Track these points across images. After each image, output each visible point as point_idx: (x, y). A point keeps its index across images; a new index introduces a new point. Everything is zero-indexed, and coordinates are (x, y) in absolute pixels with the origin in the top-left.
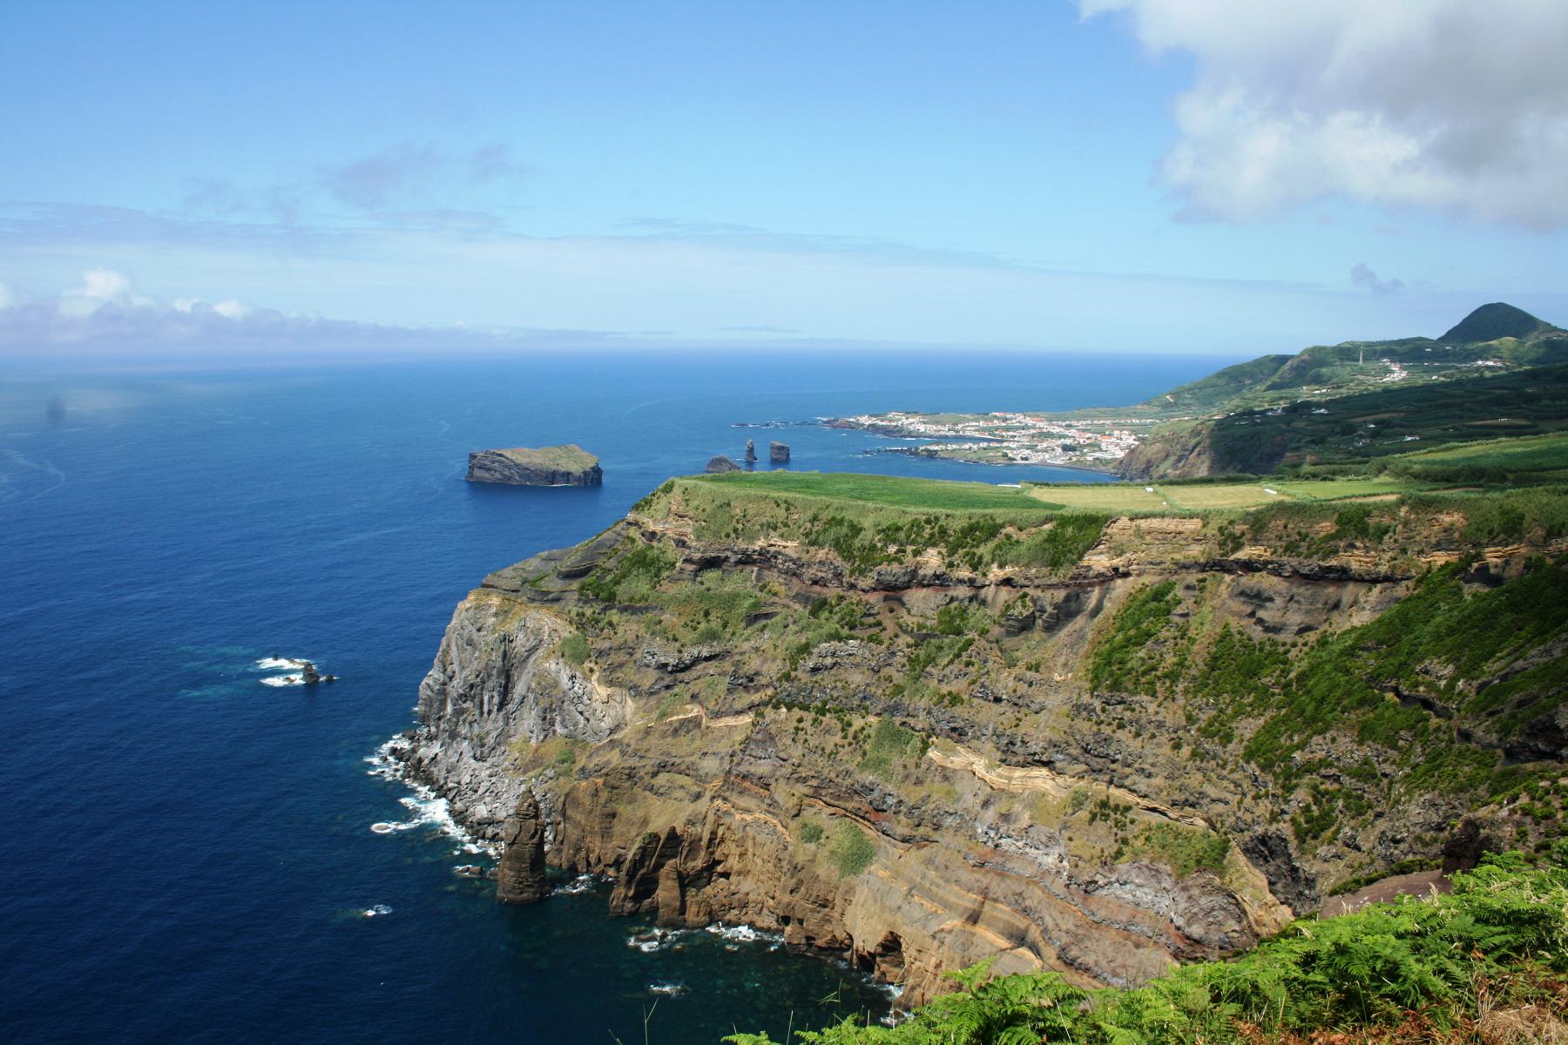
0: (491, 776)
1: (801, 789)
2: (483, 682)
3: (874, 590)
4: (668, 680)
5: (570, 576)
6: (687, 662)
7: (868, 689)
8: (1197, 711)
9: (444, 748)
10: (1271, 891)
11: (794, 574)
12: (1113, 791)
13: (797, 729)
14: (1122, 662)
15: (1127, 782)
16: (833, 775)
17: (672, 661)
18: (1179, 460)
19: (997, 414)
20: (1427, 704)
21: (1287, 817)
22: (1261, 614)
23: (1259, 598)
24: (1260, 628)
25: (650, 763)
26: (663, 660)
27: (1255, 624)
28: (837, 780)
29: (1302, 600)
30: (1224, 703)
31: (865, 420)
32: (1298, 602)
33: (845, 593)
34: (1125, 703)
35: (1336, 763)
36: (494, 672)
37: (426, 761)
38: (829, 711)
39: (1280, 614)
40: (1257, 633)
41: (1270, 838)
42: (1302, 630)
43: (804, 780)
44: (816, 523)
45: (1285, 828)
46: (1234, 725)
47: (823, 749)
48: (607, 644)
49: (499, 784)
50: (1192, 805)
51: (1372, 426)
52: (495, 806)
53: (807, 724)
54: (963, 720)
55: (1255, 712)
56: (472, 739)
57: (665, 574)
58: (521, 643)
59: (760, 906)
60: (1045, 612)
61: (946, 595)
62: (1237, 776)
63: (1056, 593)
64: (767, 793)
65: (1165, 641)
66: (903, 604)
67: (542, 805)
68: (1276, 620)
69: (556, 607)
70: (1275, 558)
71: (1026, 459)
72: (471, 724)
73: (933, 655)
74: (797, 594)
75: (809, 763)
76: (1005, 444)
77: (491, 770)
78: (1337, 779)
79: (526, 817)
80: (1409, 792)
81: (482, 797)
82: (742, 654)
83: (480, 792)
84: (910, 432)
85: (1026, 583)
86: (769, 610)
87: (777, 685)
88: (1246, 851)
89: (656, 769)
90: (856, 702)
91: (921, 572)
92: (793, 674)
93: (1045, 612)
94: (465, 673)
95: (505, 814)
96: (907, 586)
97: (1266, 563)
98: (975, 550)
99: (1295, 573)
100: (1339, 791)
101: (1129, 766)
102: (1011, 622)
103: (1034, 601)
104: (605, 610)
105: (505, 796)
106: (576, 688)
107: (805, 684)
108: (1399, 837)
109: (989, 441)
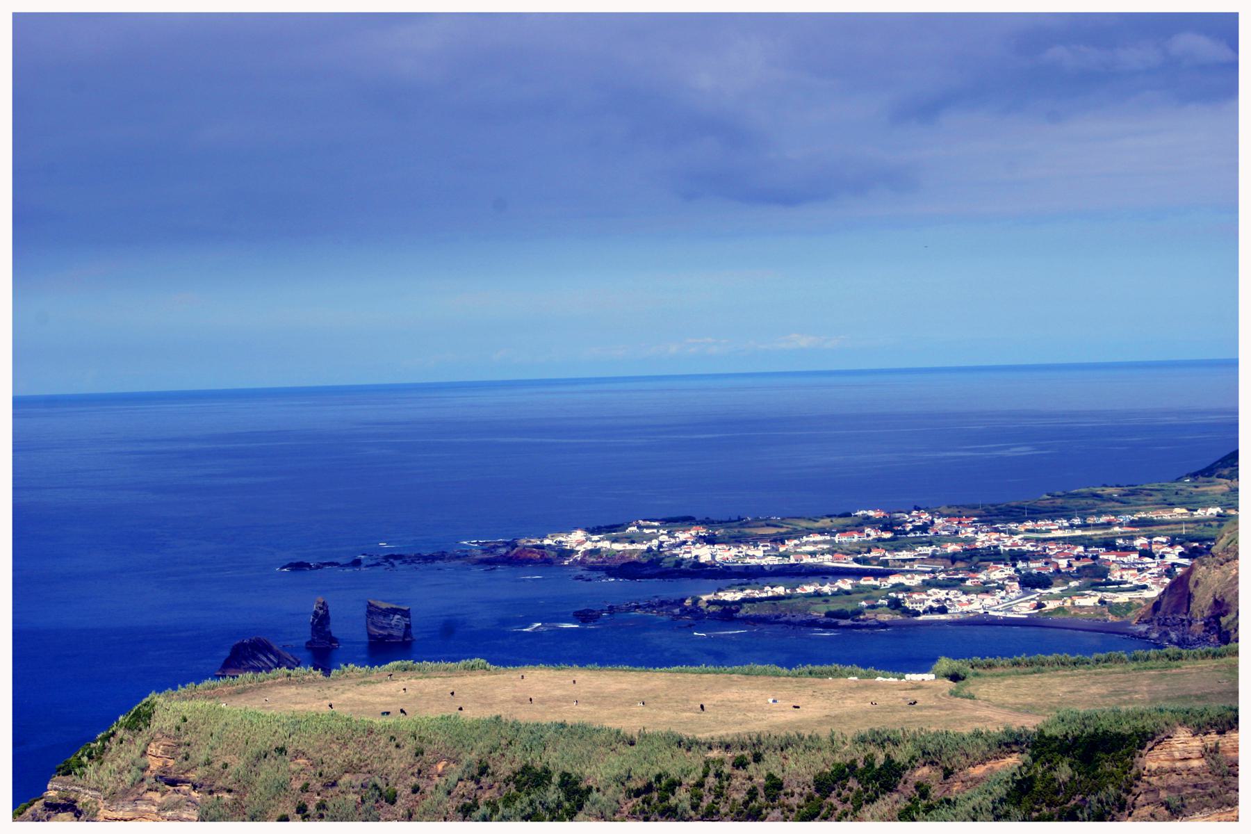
19: (871, 513)
31: (577, 541)
44: (485, 780)
71: (943, 610)
76: (893, 580)
84: (680, 562)
109: (858, 574)
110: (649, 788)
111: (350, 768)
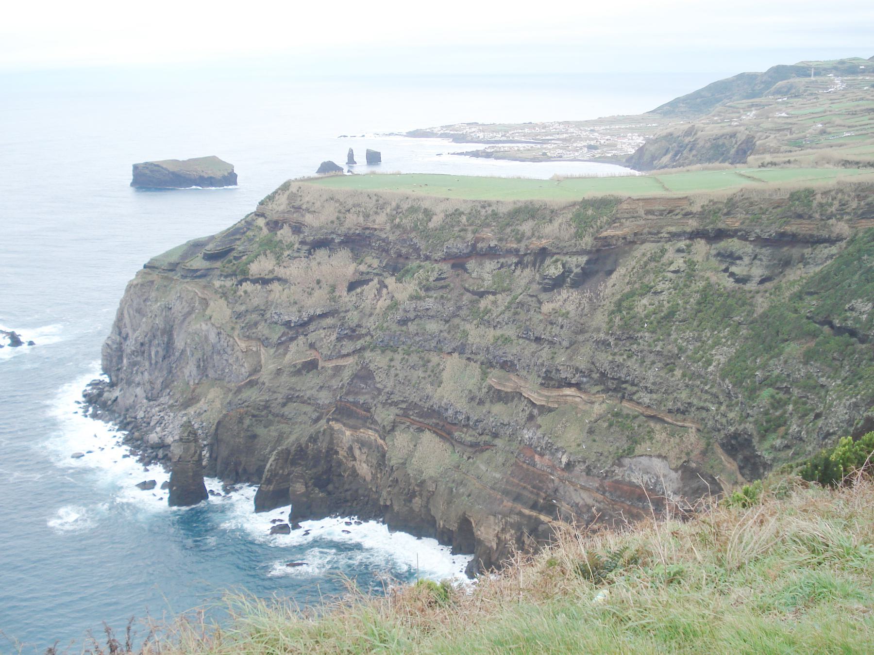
0: (160, 411)
1: (394, 410)
2: (150, 341)
3: (445, 259)
4: (291, 333)
5: (211, 257)
6: (306, 319)
7: (442, 334)
8: (685, 343)
9: (122, 392)
10: (741, 473)
11: (384, 250)
12: (625, 404)
13: (389, 366)
14: (630, 308)
15: (635, 398)
16: (417, 400)
17: (294, 319)
18: (676, 155)
20: (853, 333)
21: (751, 419)
22: (733, 269)
23: (731, 257)
24: (732, 280)
25: (280, 398)
26: (287, 318)
27: (729, 277)
28: (420, 403)
29: (763, 258)
30: (706, 336)
32: (761, 260)
33: (423, 264)
34: (632, 338)
35: (787, 379)
36: (159, 333)
37: (109, 402)
38: (412, 352)
39: (747, 269)
40: (729, 283)
41: (740, 434)
42: (762, 282)
43: (395, 404)
45: (750, 427)
46: (713, 352)
47: (409, 381)
48: (243, 308)
49: (166, 417)
50: (683, 413)
51: (820, 125)
52: (164, 433)
53: (396, 363)
54: (512, 355)
55: (729, 343)
56: (144, 384)
57: (286, 253)
58: (179, 308)
59: (367, 499)
60: (572, 272)
61: (498, 262)
62: (714, 390)
63: (580, 259)
64: (369, 414)
65: (662, 292)
66: (466, 270)
67: (200, 432)
68: (745, 273)
69: (203, 281)
70: (743, 227)
72: (142, 373)
73: (489, 307)
74: (387, 264)
75: (399, 391)
77: (159, 407)
78: (787, 391)
79: (188, 441)
80: (839, 398)
81: (154, 427)
82: (347, 311)
83: (152, 424)
85: (557, 251)
86: (367, 277)
87: (374, 333)
88: (723, 446)
89: (285, 401)
90: (433, 344)
91: (479, 245)
92: (385, 325)
93: (572, 272)
94: (137, 333)
95: (172, 440)
96: (469, 256)
97: (736, 231)
98: (519, 228)
99: (758, 237)
100: (789, 399)
101: (636, 385)
102: (546, 281)
103: (564, 266)
104: (240, 283)
105: (171, 426)
106: (222, 342)
107: (395, 332)
108: (831, 431)
110: (453, 214)
111: (354, 205)
